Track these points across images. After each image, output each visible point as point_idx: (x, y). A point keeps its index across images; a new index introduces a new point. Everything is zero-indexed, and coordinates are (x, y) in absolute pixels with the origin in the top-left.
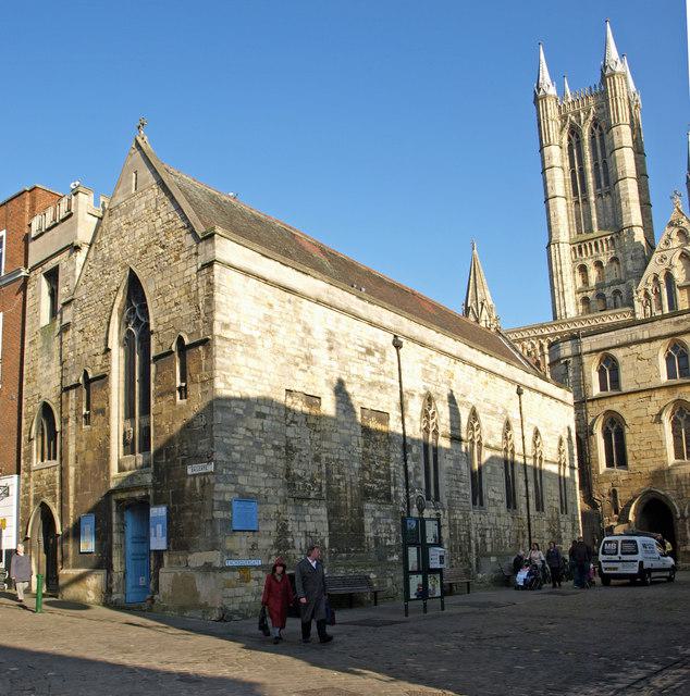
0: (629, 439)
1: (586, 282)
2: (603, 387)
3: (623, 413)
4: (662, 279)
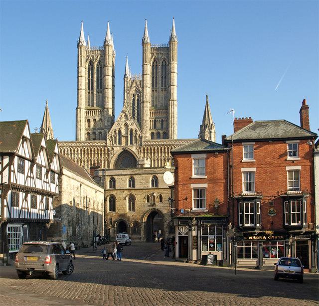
0: (118, 204)
1: (89, 126)
2: (110, 187)
3: (115, 195)
4: (117, 132)
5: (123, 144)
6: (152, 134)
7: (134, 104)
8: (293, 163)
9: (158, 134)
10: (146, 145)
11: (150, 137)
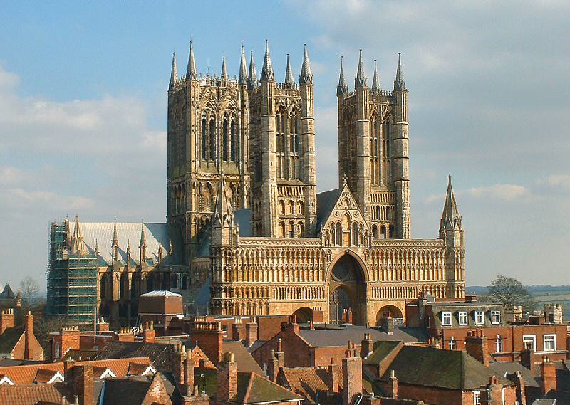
4: (335, 226)
5: (345, 245)
7: (204, 129)
9: (383, 228)
10: (375, 247)
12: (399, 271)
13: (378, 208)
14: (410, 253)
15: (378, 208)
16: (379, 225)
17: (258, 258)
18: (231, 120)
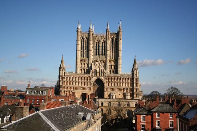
2: (101, 105)
4: (95, 70)
5: (98, 75)
6: (110, 71)
7: (96, 47)
8: (171, 119)
9: (113, 71)
10: (108, 77)
11: (109, 72)
12: (115, 84)
13: (112, 65)
14: (119, 78)
15: (112, 65)
16: (112, 70)
17: (71, 79)
18: (104, 45)
